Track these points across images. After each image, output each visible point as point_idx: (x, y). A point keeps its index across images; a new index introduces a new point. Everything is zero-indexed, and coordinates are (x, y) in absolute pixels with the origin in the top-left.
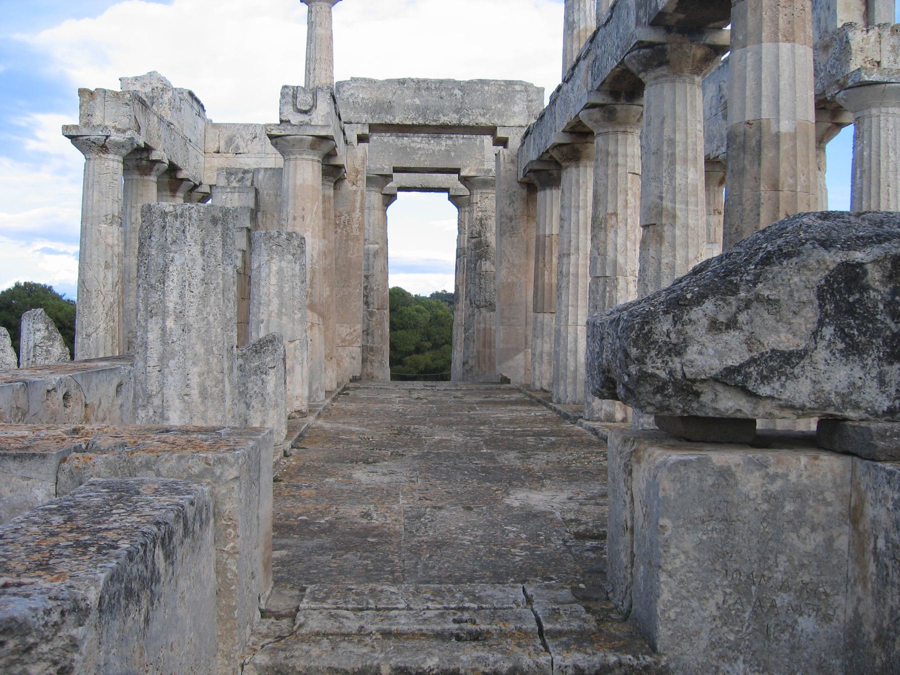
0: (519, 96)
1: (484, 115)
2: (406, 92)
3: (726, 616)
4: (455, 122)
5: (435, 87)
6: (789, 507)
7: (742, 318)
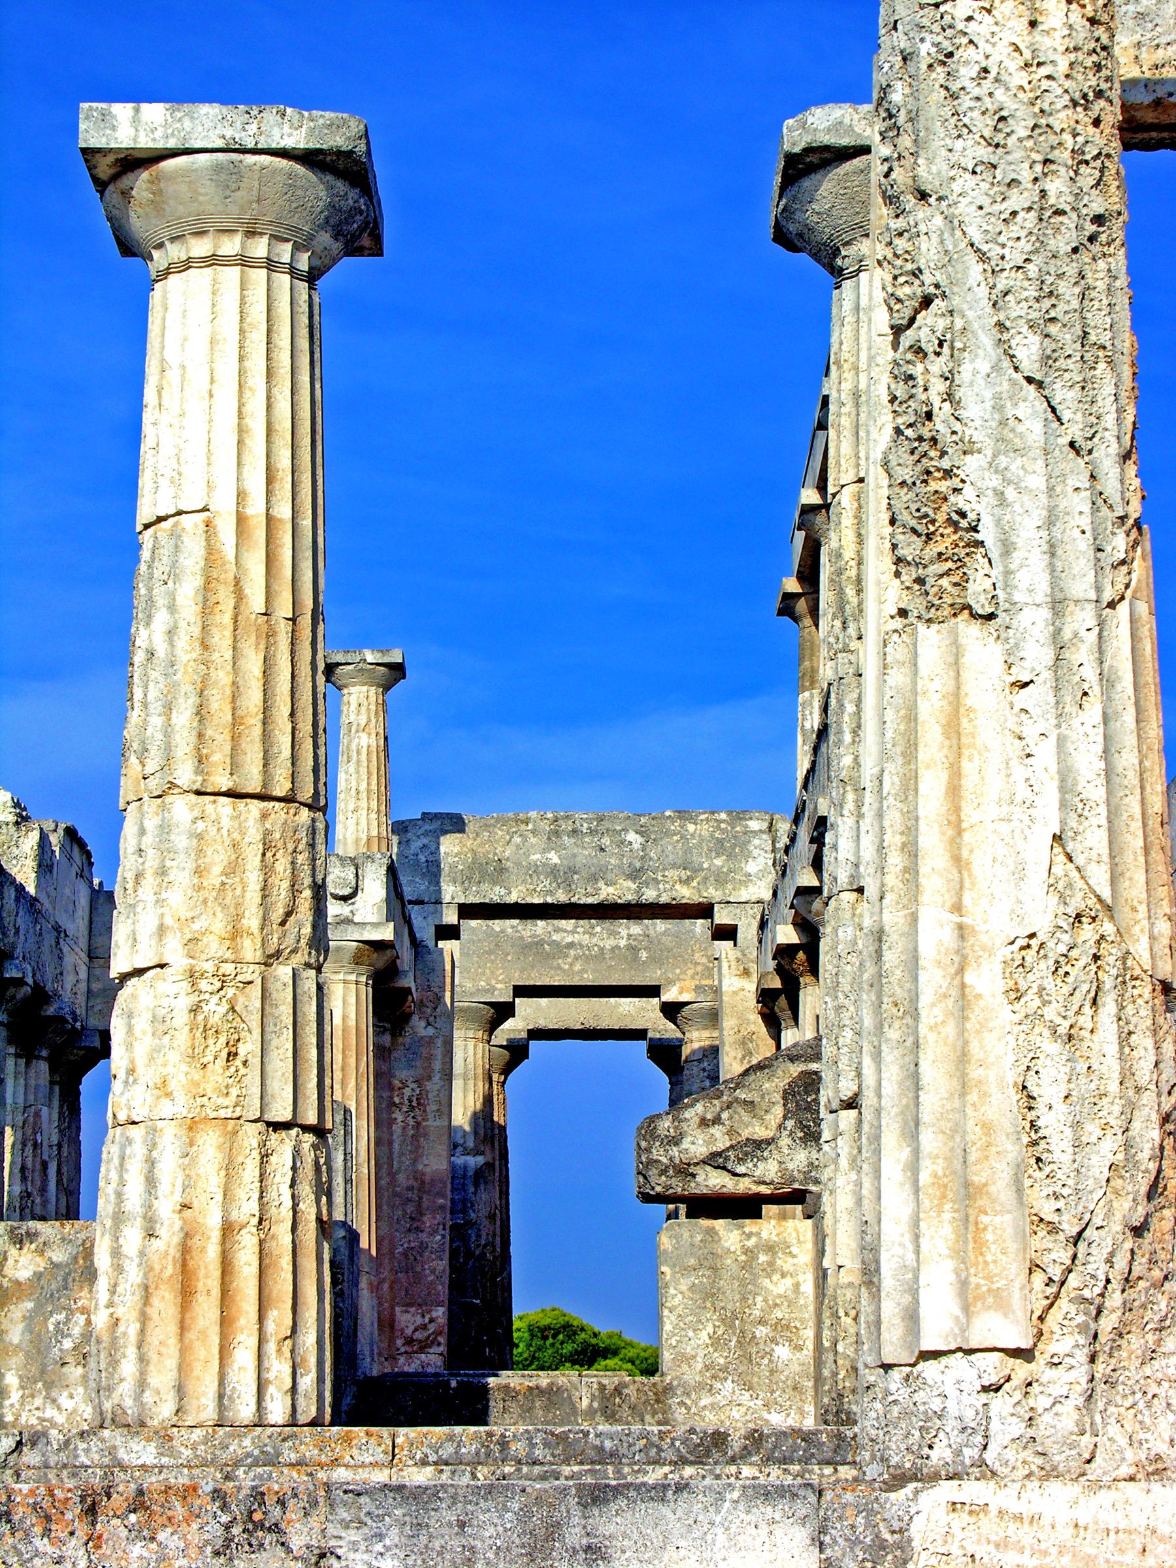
0: (756, 842)
1: (686, 882)
2: (533, 840)
3: (716, 1342)
4: (630, 897)
5: (589, 828)
6: (763, 1258)
7: (725, 1115)
